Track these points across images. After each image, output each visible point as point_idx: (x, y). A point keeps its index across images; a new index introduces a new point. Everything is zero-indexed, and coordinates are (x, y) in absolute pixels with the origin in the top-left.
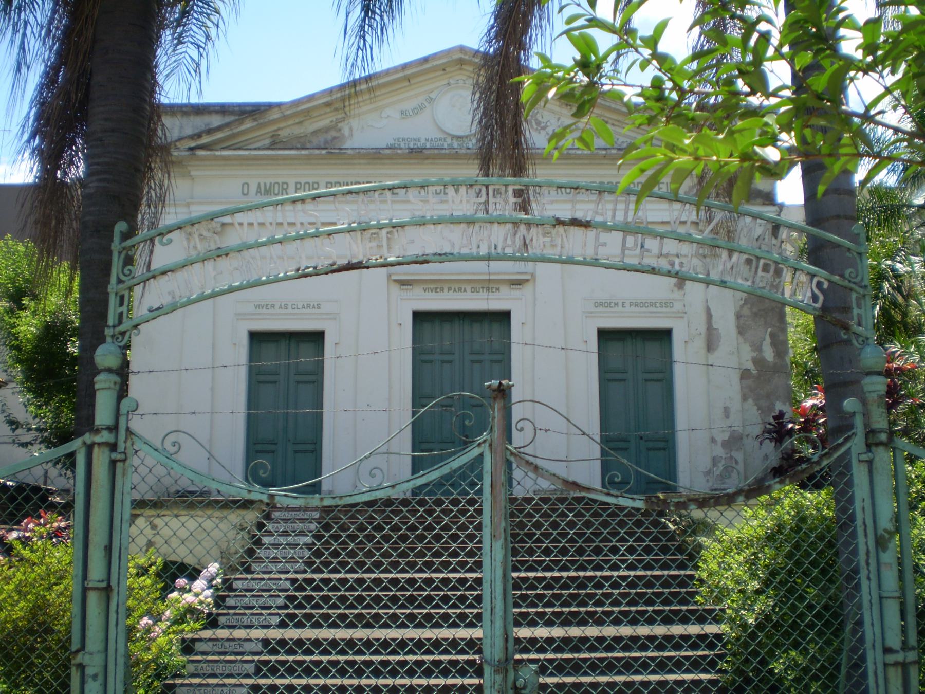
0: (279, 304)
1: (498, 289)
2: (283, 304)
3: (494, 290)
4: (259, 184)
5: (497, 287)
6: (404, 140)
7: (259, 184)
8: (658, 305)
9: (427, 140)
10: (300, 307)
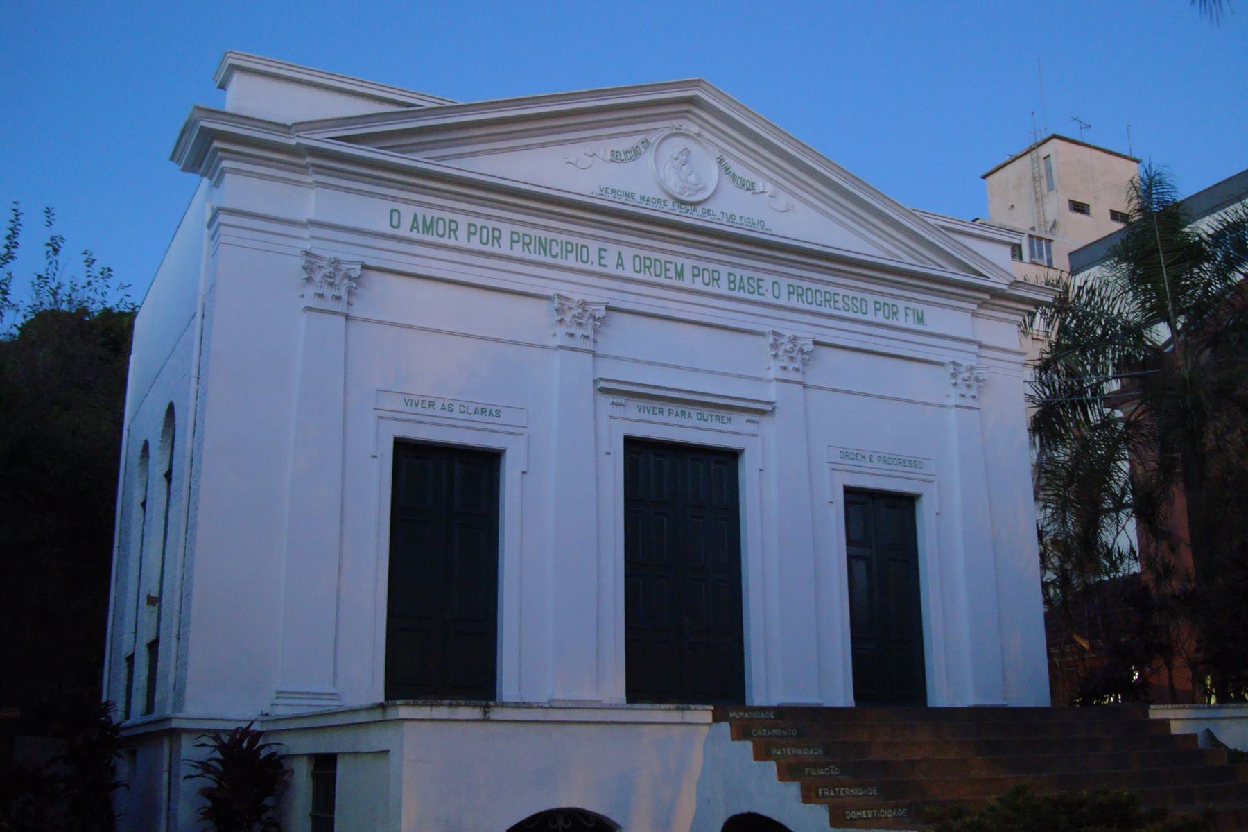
0: (441, 402)
1: (729, 419)
2: (446, 405)
3: (725, 420)
4: (415, 215)
5: (729, 416)
6: (613, 191)
7: (415, 215)
8: (907, 464)
9: (642, 198)
10: (472, 410)
